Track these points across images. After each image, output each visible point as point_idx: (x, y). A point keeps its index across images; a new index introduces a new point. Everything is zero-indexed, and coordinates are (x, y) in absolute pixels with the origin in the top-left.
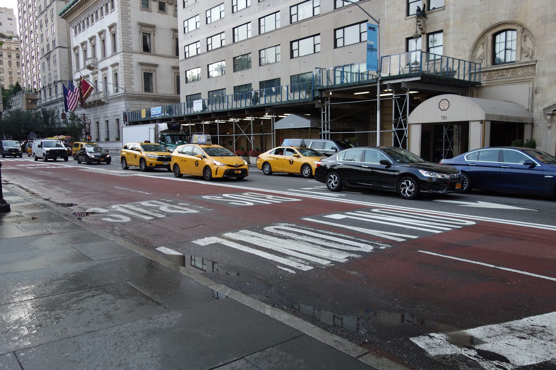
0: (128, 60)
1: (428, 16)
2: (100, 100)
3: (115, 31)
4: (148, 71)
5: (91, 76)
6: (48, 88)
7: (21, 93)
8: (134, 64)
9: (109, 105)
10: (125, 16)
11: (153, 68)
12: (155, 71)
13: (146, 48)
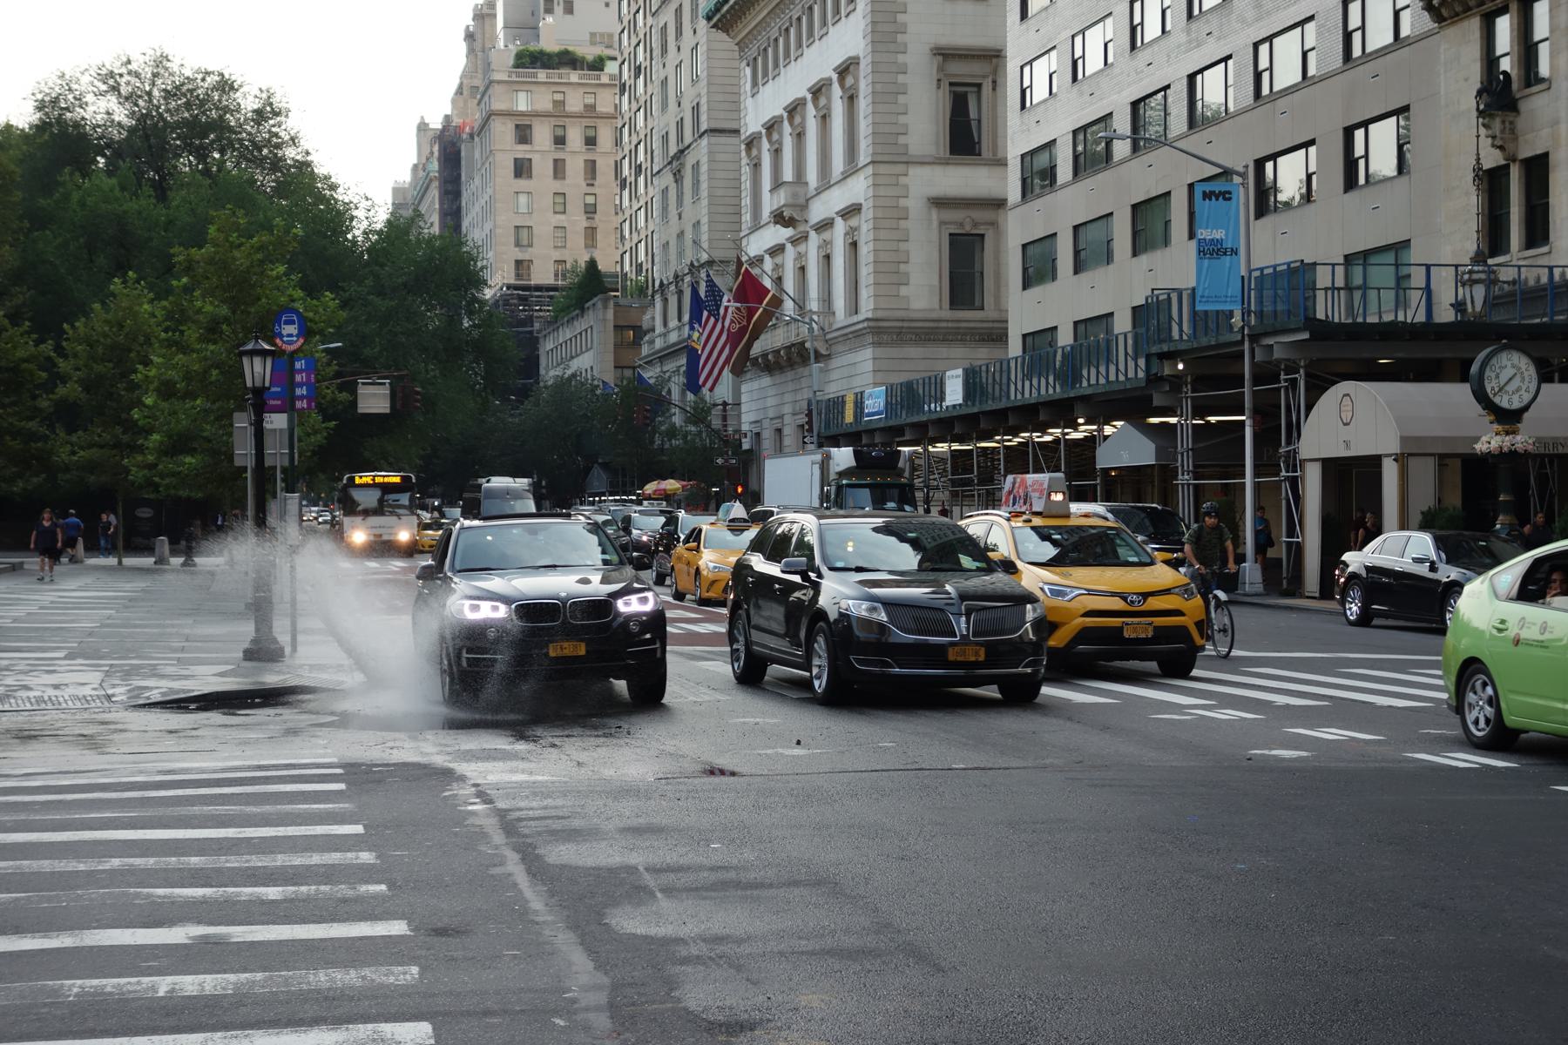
0: (891, 192)
1: (1523, 106)
3: (855, 87)
4: (968, 229)
6: (672, 288)
7: (600, 305)
8: (915, 203)
9: (835, 363)
10: (885, 33)
12: (994, 224)
13: (964, 138)
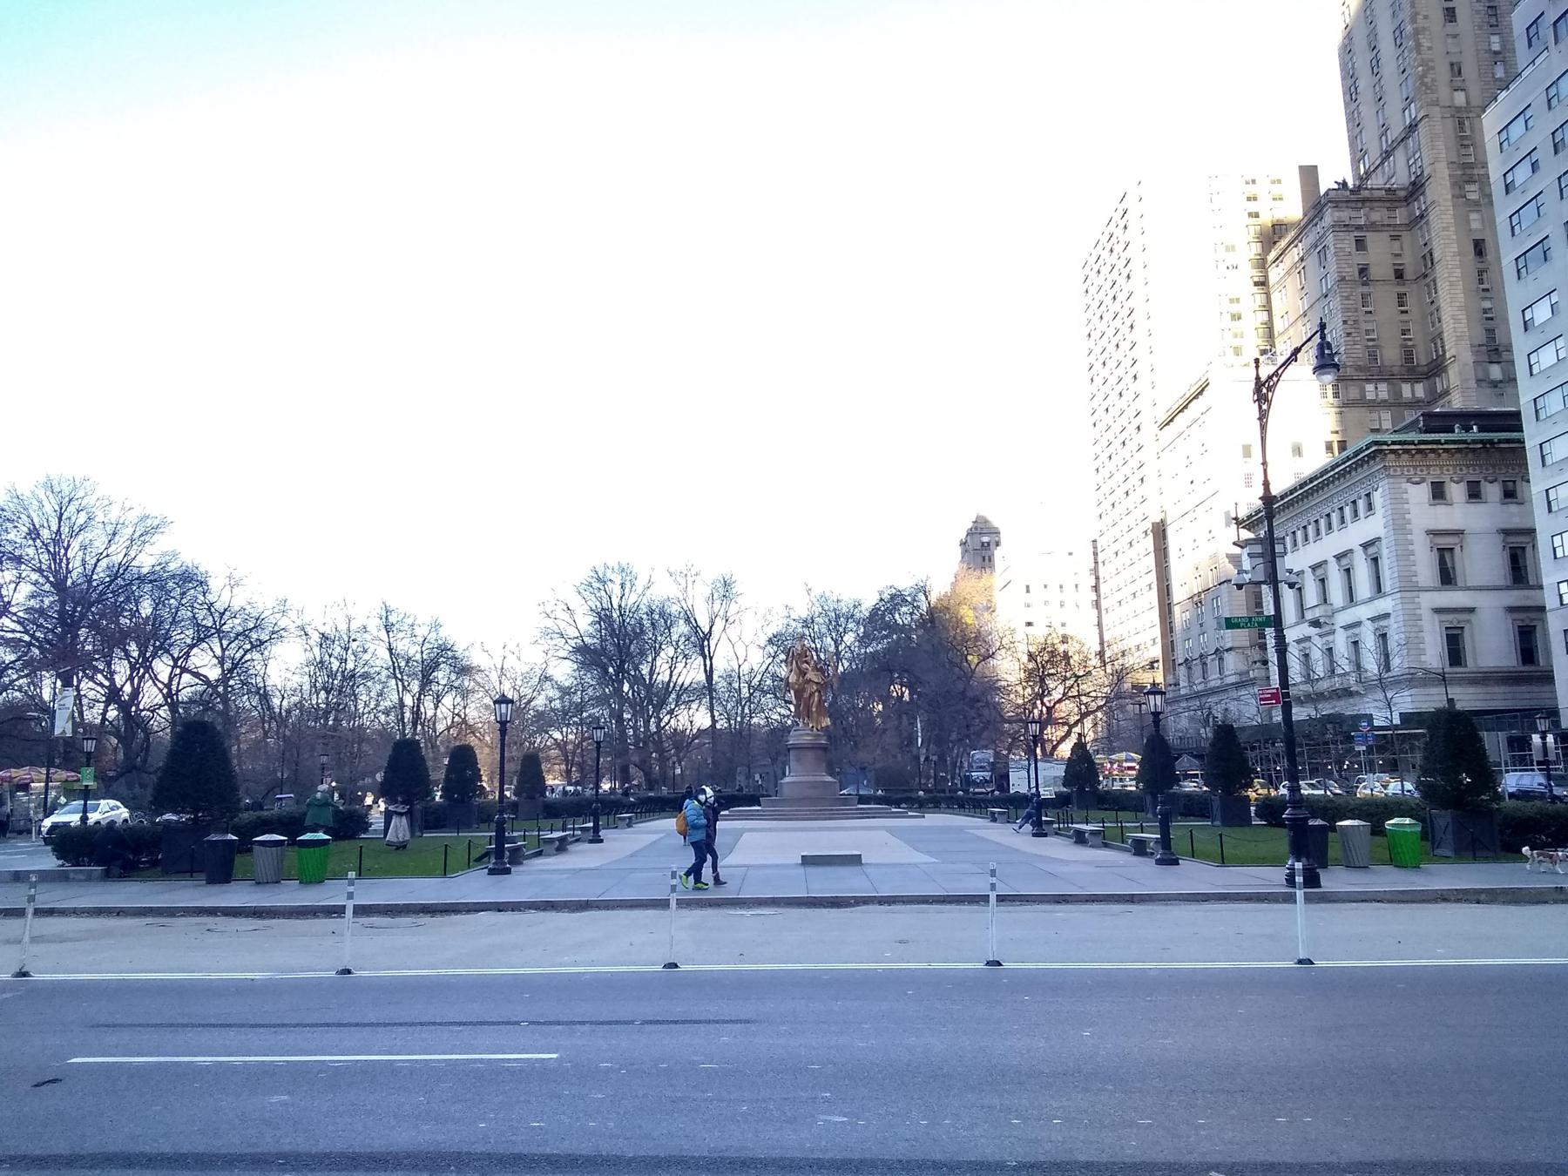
2: (1345, 690)
5: (1317, 640)
8: (1426, 614)
10: (1400, 524)
11: (1465, 616)
12: (1469, 621)
13: (1447, 577)
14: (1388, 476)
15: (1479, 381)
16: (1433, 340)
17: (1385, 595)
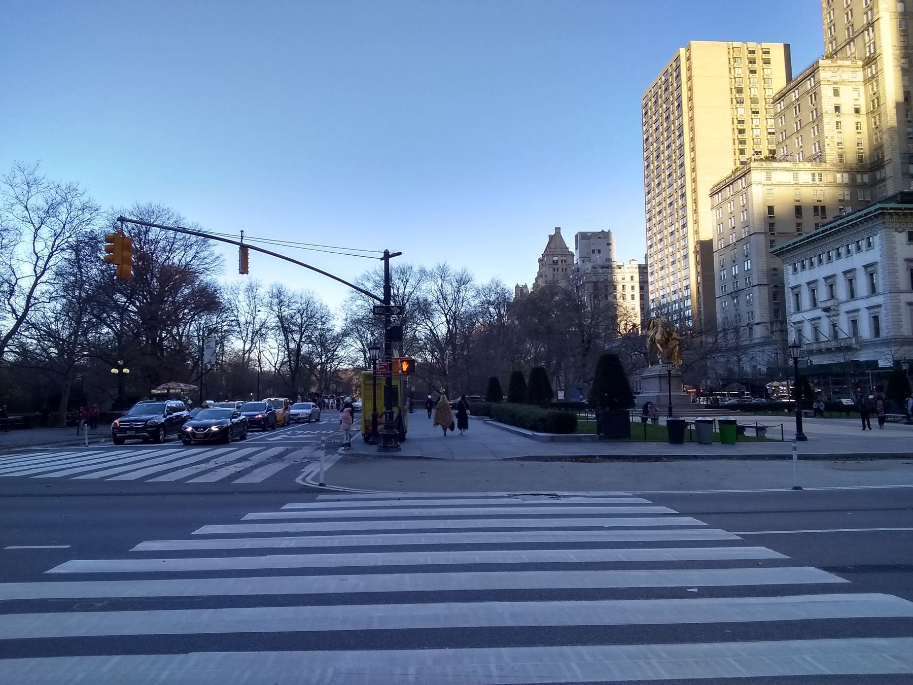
8: (903, 305)
10: (890, 254)
14: (885, 227)
15: (904, 174)
16: (876, 150)
17: (878, 294)
